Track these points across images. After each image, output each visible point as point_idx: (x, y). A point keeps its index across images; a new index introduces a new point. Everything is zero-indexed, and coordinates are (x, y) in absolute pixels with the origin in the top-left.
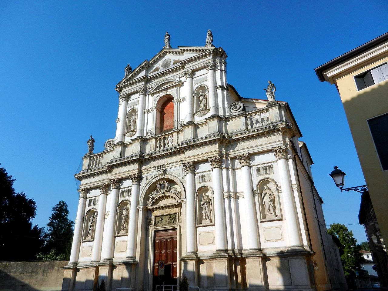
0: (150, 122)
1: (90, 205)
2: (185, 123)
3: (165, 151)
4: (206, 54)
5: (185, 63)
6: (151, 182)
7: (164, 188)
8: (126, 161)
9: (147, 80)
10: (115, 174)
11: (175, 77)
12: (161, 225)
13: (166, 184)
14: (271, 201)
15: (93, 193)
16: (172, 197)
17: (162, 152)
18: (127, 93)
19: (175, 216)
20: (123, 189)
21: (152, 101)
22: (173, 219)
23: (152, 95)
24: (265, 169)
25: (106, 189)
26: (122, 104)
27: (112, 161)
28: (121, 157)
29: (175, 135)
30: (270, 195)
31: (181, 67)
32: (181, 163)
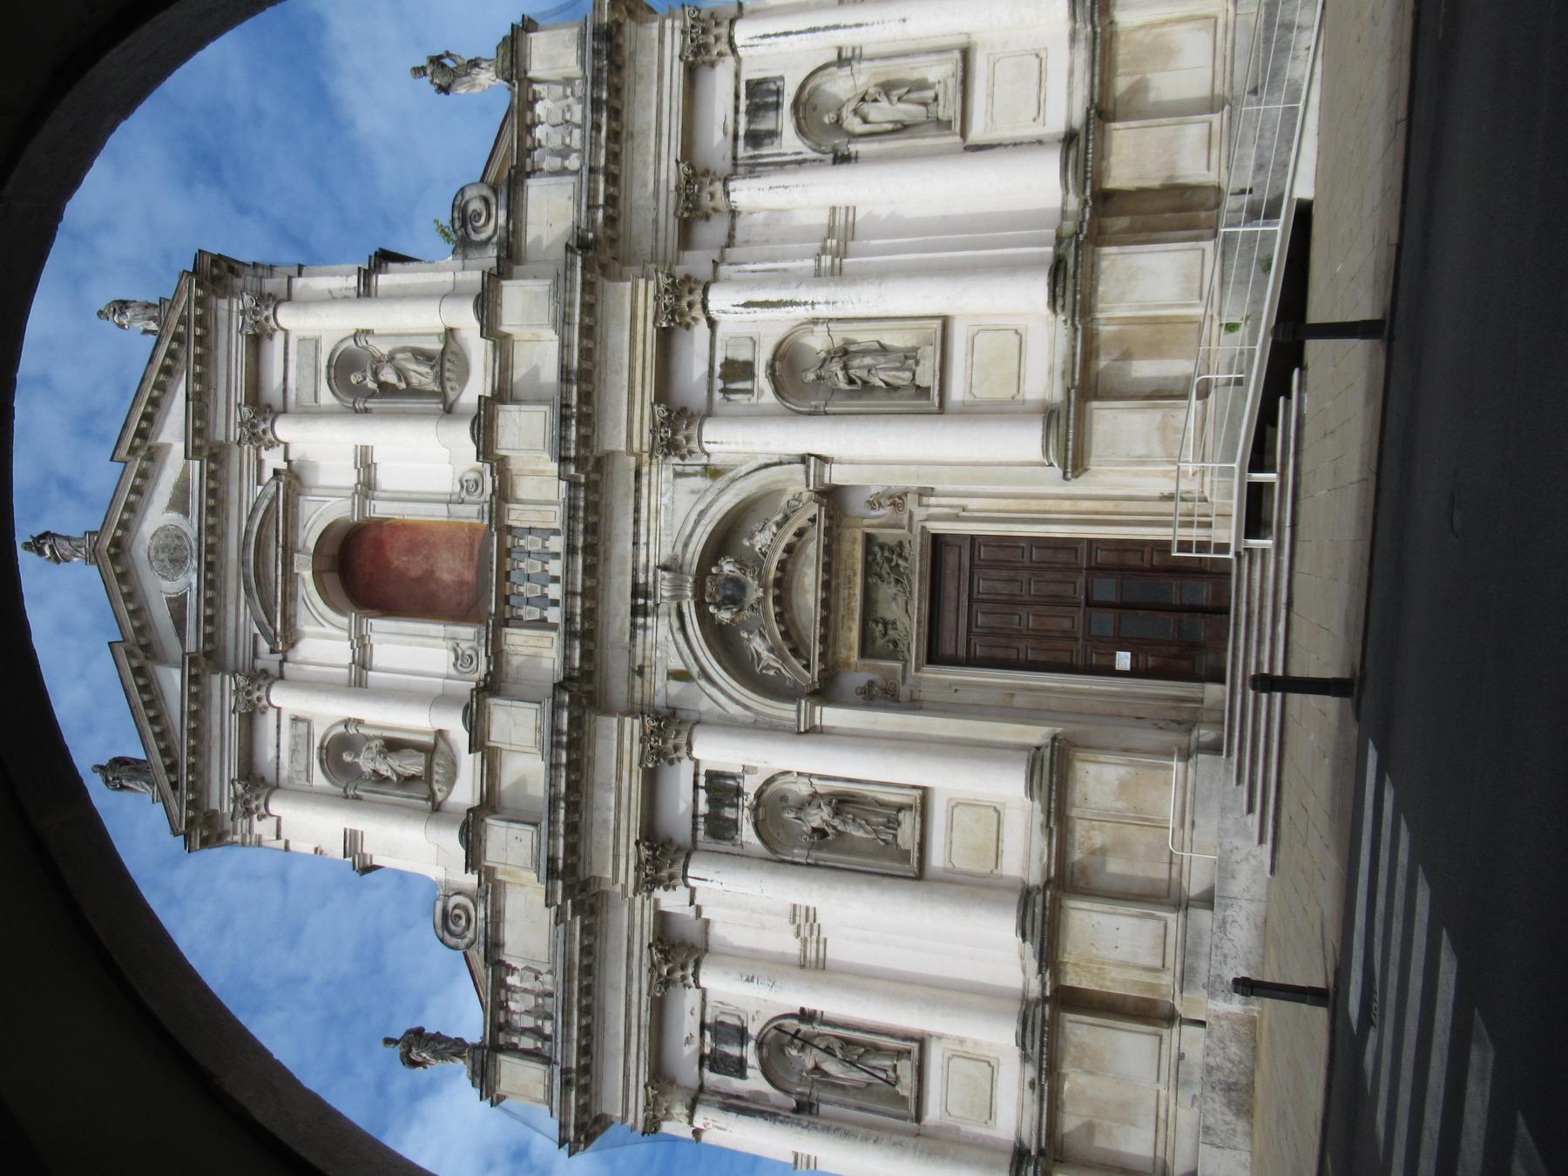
0: (418, 651)
1: (739, 1068)
3: (571, 550)
4: (200, 321)
6: (700, 654)
7: (739, 586)
9: (208, 660)
11: (247, 494)
12: (907, 622)
13: (728, 567)
14: (887, 95)
15: (685, 1049)
16: (789, 549)
17: (575, 572)
18: (234, 774)
19: (877, 549)
21: (324, 638)
22: (889, 560)
23: (290, 637)
24: (755, 111)
25: (678, 950)
26: (279, 819)
29: (517, 516)
30: (863, 100)
31: (213, 466)
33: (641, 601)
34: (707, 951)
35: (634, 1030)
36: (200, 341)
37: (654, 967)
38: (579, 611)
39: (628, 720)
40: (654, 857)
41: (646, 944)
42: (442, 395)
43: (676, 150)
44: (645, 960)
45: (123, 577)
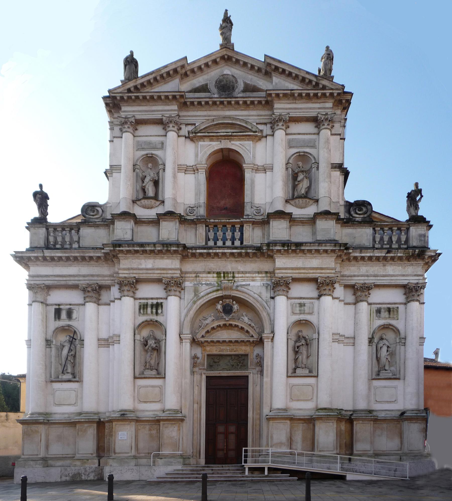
20: (145, 301)
32: (264, 275)
34: (99, 305)
35: (64, 279)
37: (89, 285)
40: (130, 284)
41: (98, 282)
42: (293, 198)
43: (378, 282)
44: (92, 282)
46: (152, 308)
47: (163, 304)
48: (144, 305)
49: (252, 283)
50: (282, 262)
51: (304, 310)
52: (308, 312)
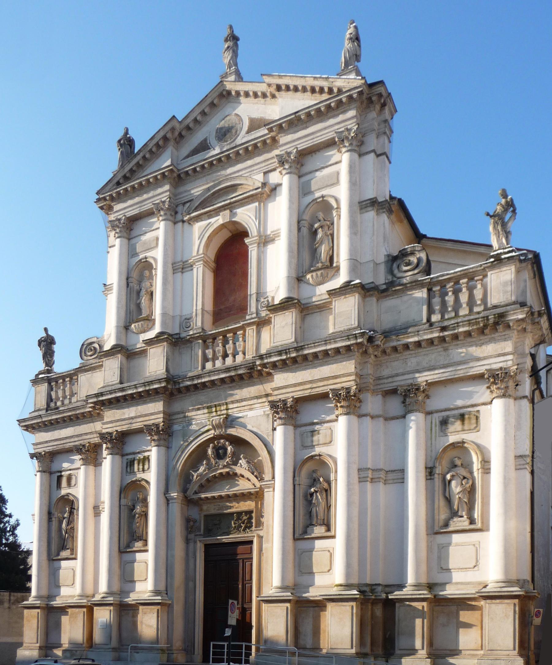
2: (277, 302)
5: (280, 126)
8: (134, 391)
10: (111, 422)
17: (219, 374)
27: (103, 390)
28: (121, 383)
32: (264, 400)
33: (214, 409)
36: (340, 102)
38: (203, 380)
39: (161, 415)
45: (213, 105)
46: (139, 465)
47: (150, 458)
48: (131, 462)
49: (250, 414)
50: (281, 379)
51: (319, 440)
52: (324, 442)
